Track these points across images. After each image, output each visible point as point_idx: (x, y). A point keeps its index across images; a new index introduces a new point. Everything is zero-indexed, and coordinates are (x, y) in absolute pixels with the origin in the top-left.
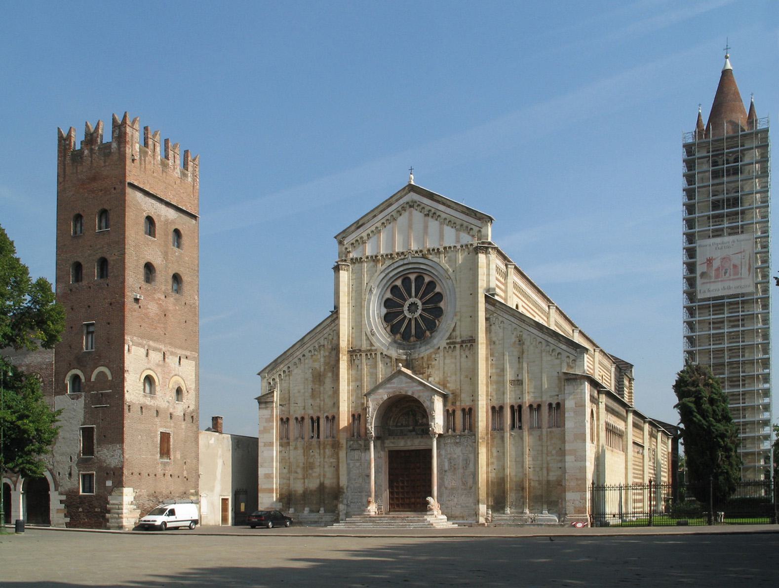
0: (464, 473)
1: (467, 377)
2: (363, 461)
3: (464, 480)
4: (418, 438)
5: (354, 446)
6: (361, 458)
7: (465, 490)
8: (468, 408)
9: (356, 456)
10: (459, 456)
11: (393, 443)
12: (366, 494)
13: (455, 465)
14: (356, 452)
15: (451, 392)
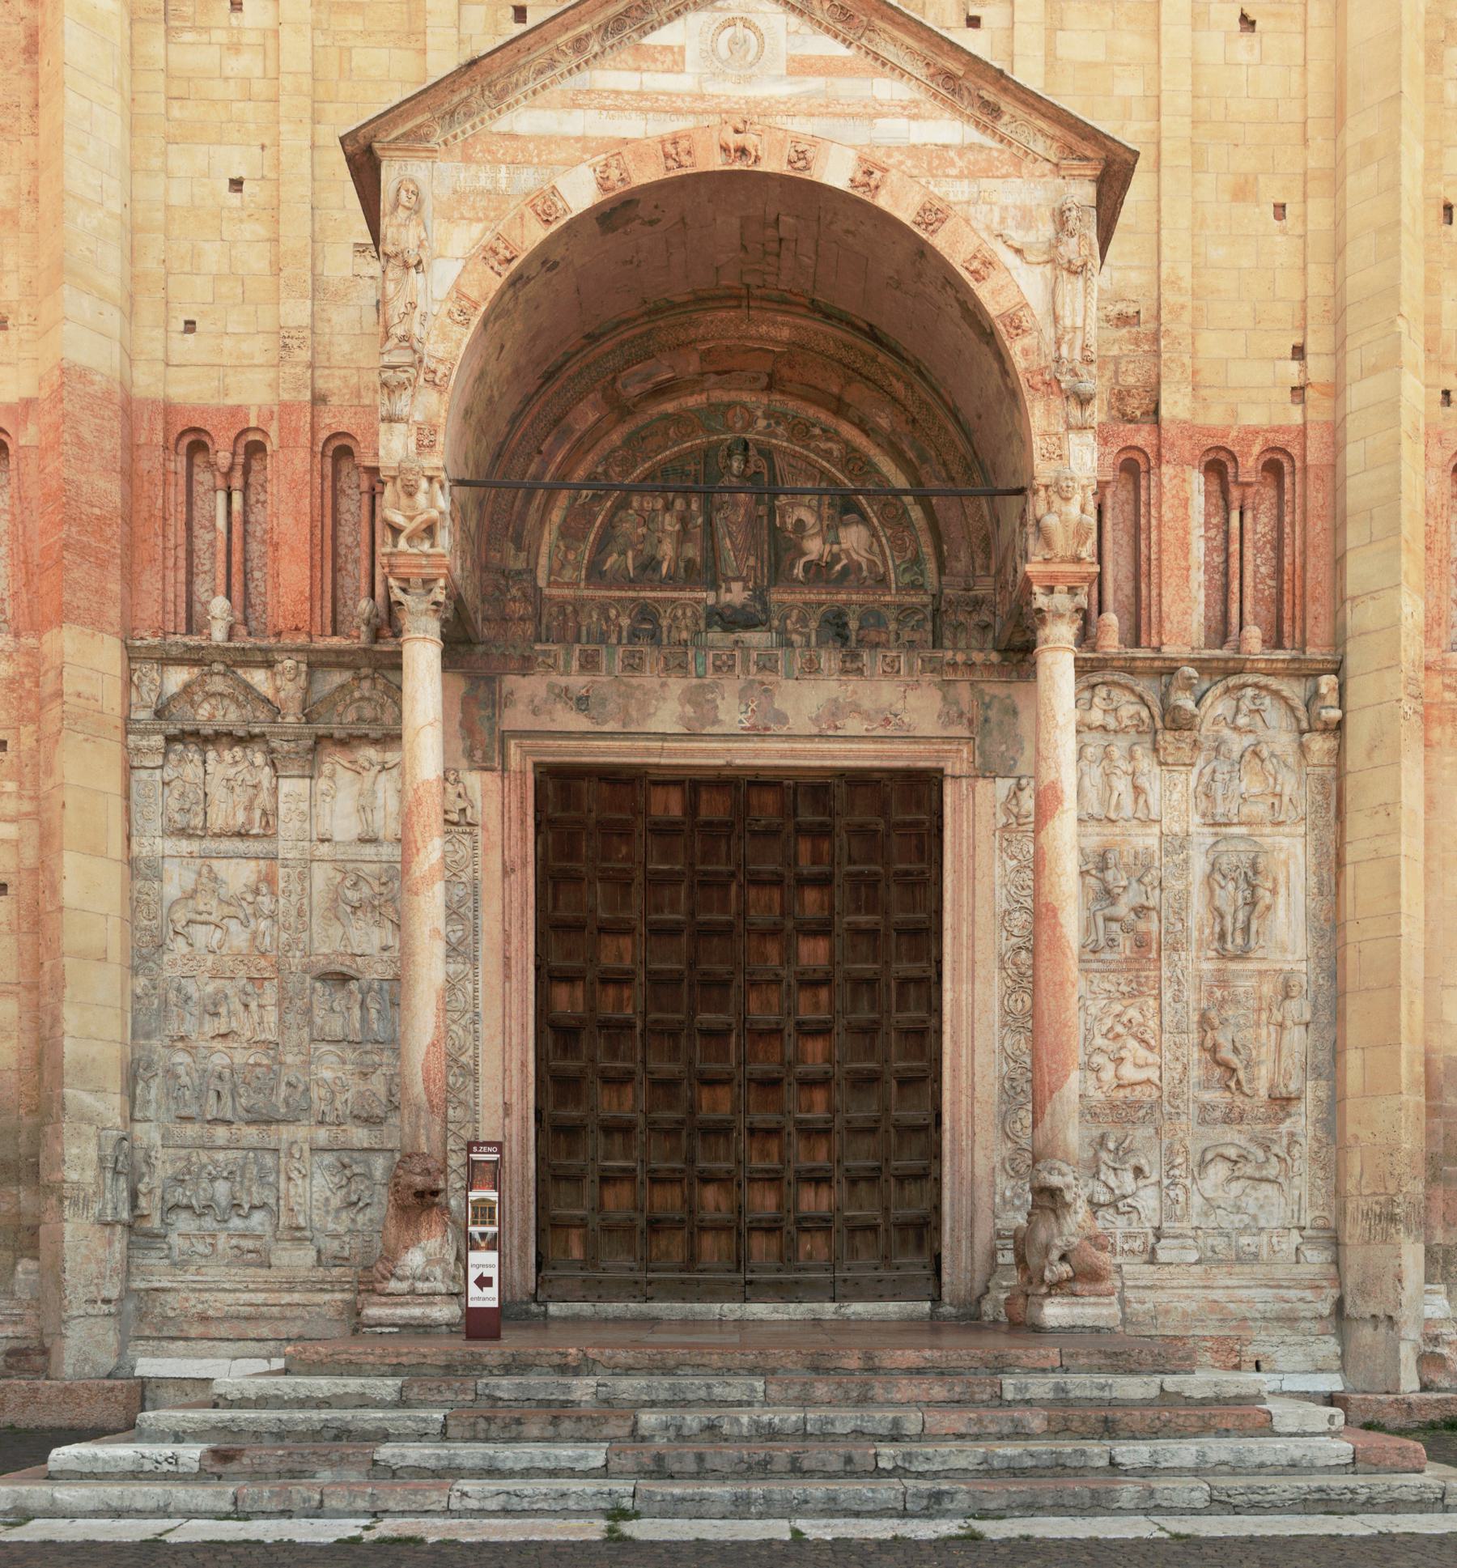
0: (1222, 980)
1: (1242, 191)
2: (285, 848)
3: (1224, 1039)
4: (812, 668)
5: (204, 711)
6: (269, 816)
7: (1227, 1120)
8: (1256, 449)
9: (217, 791)
10: (1181, 843)
11: (582, 703)
12: (322, 1135)
13: (1141, 911)
14: (223, 764)
15: (1113, 310)
